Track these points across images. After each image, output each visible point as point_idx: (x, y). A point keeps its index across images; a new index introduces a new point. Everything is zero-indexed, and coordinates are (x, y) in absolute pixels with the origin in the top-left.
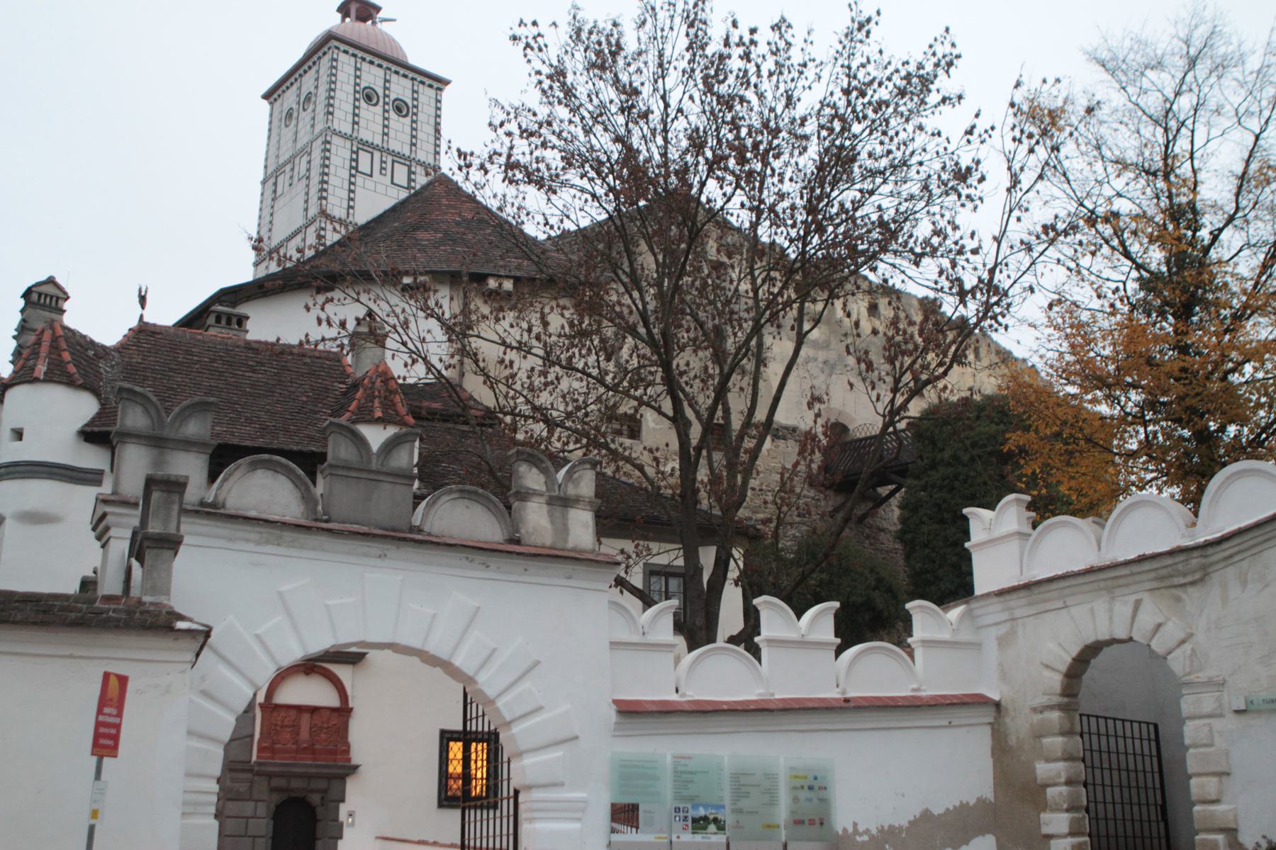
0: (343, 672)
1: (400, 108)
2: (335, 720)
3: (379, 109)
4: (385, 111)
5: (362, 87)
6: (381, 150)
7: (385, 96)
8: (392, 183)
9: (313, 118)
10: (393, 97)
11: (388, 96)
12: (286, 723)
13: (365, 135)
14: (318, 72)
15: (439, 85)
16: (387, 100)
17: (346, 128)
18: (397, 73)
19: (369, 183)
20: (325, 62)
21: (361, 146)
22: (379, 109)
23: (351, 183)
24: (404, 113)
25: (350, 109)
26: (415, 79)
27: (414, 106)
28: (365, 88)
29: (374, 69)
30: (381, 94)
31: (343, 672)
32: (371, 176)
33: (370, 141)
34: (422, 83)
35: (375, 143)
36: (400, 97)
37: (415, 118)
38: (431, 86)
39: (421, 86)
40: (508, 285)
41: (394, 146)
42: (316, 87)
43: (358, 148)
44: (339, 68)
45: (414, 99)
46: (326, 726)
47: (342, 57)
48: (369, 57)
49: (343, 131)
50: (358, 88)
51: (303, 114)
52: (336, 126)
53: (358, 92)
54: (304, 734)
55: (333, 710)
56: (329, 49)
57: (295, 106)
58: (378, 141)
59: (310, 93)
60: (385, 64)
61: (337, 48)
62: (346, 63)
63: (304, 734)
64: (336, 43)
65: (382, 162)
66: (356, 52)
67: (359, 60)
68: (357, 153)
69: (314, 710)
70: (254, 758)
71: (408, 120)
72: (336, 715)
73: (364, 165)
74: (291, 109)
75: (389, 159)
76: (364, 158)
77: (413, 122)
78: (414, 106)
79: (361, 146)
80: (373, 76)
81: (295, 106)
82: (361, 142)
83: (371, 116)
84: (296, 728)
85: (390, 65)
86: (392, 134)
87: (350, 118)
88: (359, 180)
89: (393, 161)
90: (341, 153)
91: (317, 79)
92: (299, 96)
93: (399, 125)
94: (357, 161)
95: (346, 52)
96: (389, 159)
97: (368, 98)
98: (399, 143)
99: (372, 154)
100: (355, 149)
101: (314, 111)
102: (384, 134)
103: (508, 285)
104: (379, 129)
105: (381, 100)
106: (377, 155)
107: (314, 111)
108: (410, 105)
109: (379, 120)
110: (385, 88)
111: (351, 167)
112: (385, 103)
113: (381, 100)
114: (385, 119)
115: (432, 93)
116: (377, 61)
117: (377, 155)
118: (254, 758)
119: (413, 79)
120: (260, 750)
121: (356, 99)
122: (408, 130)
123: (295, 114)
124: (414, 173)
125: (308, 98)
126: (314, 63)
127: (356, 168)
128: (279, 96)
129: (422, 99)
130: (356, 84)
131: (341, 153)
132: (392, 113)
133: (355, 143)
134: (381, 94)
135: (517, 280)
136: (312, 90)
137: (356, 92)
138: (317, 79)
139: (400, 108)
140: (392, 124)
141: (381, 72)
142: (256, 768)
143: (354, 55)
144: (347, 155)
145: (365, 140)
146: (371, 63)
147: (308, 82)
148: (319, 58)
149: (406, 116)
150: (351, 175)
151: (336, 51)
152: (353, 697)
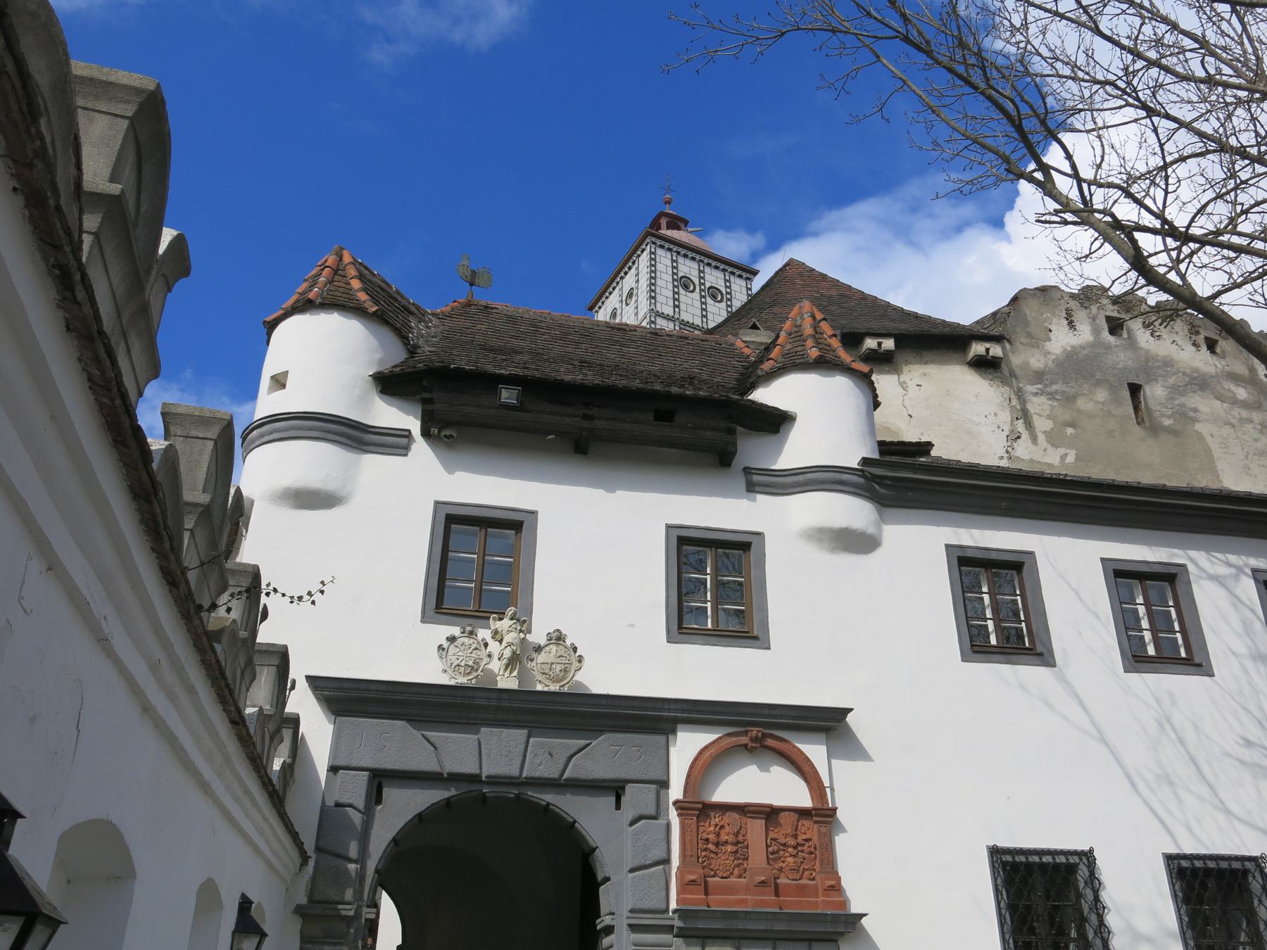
0: (815, 752)
1: (714, 293)
2: (809, 829)
3: (696, 295)
4: (702, 297)
5: (679, 276)
7: (701, 284)
9: (637, 308)
10: (708, 285)
11: (704, 284)
12: (724, 837)
14: (637, 268)
15: (748, 275)
16: (703, 287)
17: (669, 311)
18: (709, 265)
20: (644, 259)
21: (683, 327)
24: (719, 298)
25: (670, 294)
26: (727, 270)
27: (727, 293)
28: (682, 277)
29: (689, 263)
30: (696, 281)
31: (815, 752)
33: (691, 321)
34: (733, 273)
35: (696, 323)
36: (714, 285)
37: (729, 303)
38: (740, 276)
39: (732, 277)
42: (637, 281)
44: (658, 260)
45: (726, 287)
46: (792, 842)
47: (660, 252)
48: (683, 252)
49: (666, 313)
50: (675, 277)
51: (626, 309)
52: (659, 308)
53: (676, 280)
54: (757, 856)
55: (802, 813)
56: (646, 245)
57: (618, 306)
59: (632, 289)
60: (698, 257)
61: (654, 243)
63: (757, 856)
64: (654, 239)
66: (672, 246)
67: (674, 254)
69: (770, 814)
70: (673, 905)
71: (723, 305)
72: (806, 823)
74: (615, 309)
79: (683, 327)
80: (688, 268)
81: (618, 306)
84: (740, 845)
91: (637, 275)
92: (621, 296)
95: (662, 247)
97: (686, 287)
101: (636, 301)
102: (703, 316)
104: (699, 312)
105: (698, 288)
107: (636, 301)
108: (724, 293)
110: (700, 278)
112: (701, 290)
113: (698, 288)
114: (702, 303)
115: (743, 283)
116: (690, 254)
118: (673, 905)
119: (724, 270)
120: (685, 886)
121: (674, 286)
123: (619, 312)
125: (630, 295)
126: (634, 263)
128: (603, 303)
129: (733, 287)
132: (708, 299)
133: (677, 323)
134: (696, 281)
136: (634, 285)
138: (637, 275)
140: (709, 308)
141: (695, 265)
142: (678, 923)
143: (669, 250)
145: (686, 320)
146: (685, 256)
147: (628, 282)
148: (639, 256)
149: (721, 301)
151: (653, 246)
152: (832, 790)
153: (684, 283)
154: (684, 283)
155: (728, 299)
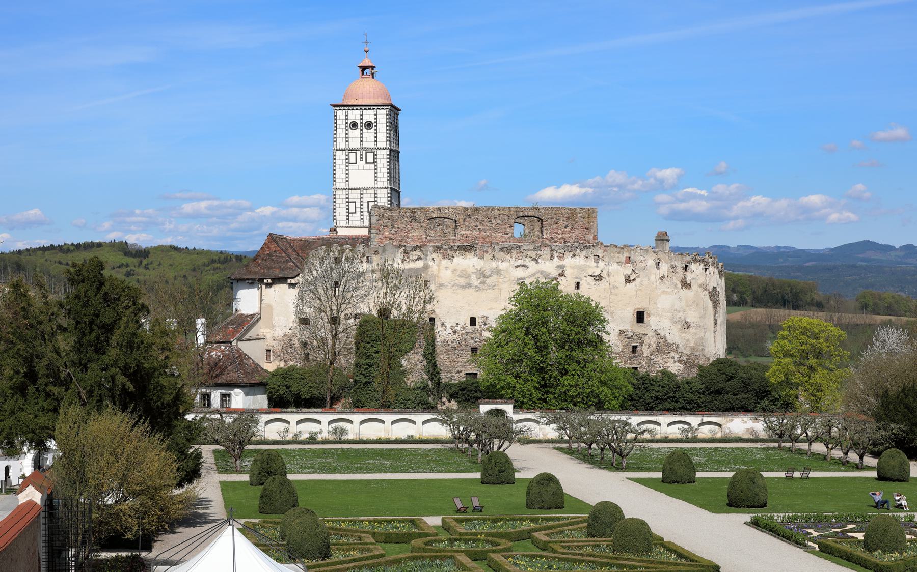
1: (369, 125)
6: (357, 150)
8: (366, 163)
13: (352, 146)
19: (355, 167)
22: (358, 130)
23: (347, 170)
30: (359, 123)
32: (356, 163)
40: (270, 281)
41: (366, 145)
43: (349, 153)
47: (339, 112)
52: (338, 147)
58: (358, 146)
60: (359, 108)
62: (341, 114)
65: (361, 155)
68: (348, 155)
73: (352, 160)
75: (364, 152)
76: (352, 156)
77: (375, 130)
78: (375, 122)
80: (354, 115)
82: (350, 149)
83: (355, 134)
85: (361, 108)
86: (365, 140)
87: (344, 140)
88: (350, 167)
89: (366, 152)
90: (341, 157)
93: (369, 134)
94: (348, 159)
96: (364, 152)
98: (369, 143)
99: (356, 153)
100: (347, 154)
103: (270, 281)
106: (358, 152)
109: (359, 135)
110: (361, 119)
111: (347, 163)
116: (355, 108)
117: (358, 152)
121: (347, 130)
122: (373, 135)
124: (376, 155)
127: (349, 163)
130: (347, 123)
131: (341, 157)
132: (365, 130)
135: (272, 279)
137: (347, 127)
139: (369, 125)
140: (365, 135)
141: (358, 112)
143: (344, 110)
144: (344, 157)
146: (353, 109)
150: (347, 166)
153: (354, 125)
154: (354, 125)
155: (375, 126)
